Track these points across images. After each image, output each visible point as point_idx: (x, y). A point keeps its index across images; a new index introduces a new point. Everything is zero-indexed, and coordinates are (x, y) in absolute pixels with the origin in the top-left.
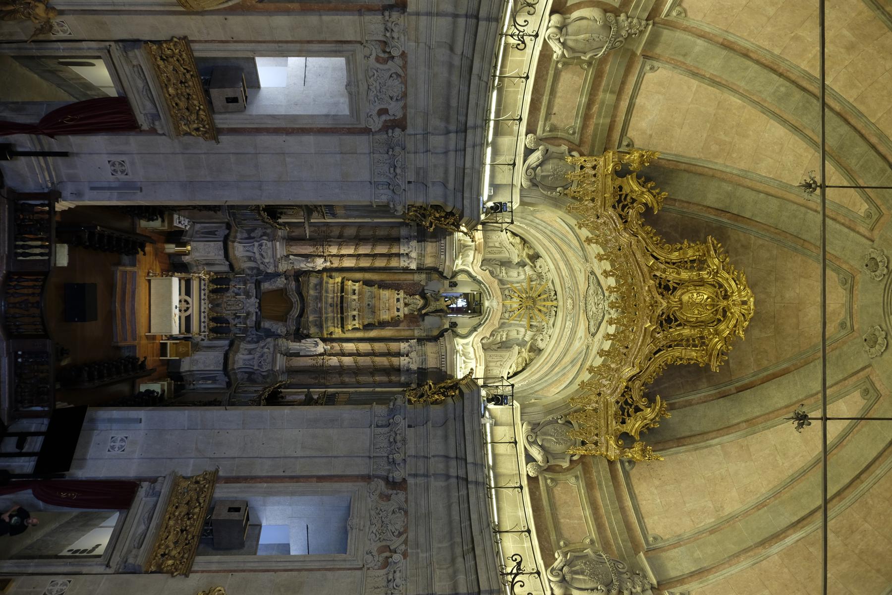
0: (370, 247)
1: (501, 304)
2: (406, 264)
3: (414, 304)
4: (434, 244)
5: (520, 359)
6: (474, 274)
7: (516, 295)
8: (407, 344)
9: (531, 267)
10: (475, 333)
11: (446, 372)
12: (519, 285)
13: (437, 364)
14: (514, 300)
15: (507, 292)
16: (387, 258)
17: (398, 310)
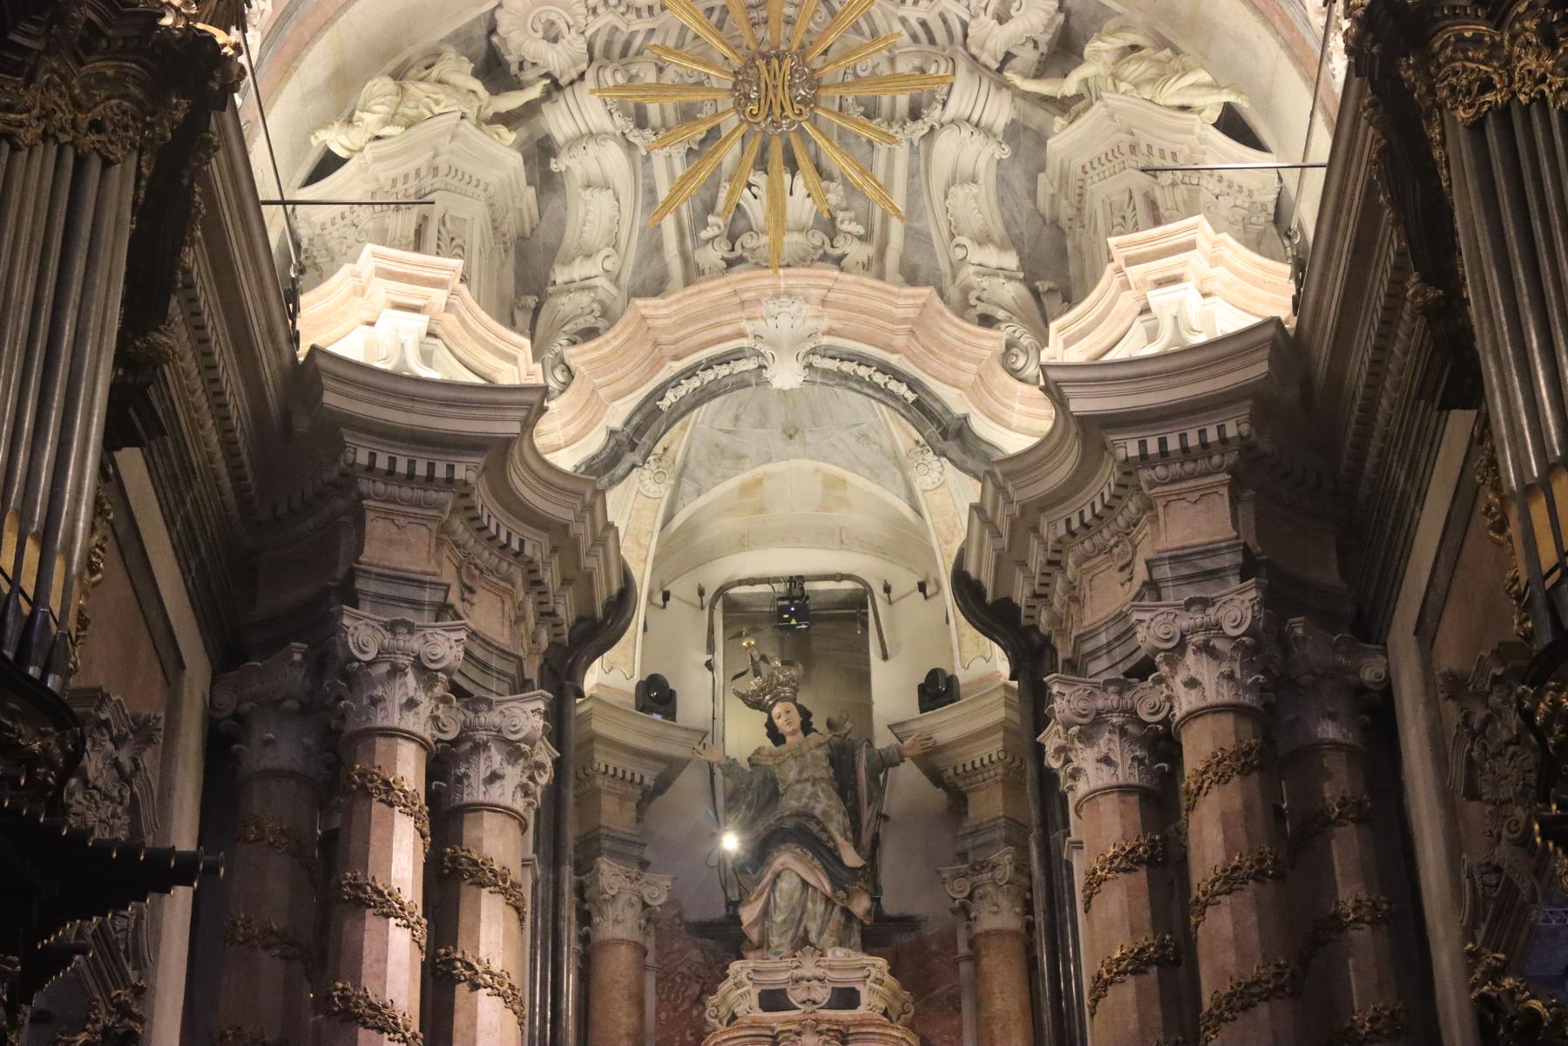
0: (371, 921)
1: (786, 279)
2: (514, 775)
3: (798, 915)
4: (376, 528)
5: (1134, 69)
6: (595, 442)
7: (723, 195)
8: (1086, 757)
9: (548, 95)
10: (982, 426)
11: (1257, 399)
12: (658, 159)
13: (1205, 491)
14: (757, 210)
15: (713, 255)
16: (466, 890)
17: (846, 998)
